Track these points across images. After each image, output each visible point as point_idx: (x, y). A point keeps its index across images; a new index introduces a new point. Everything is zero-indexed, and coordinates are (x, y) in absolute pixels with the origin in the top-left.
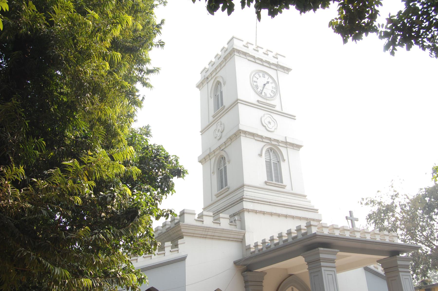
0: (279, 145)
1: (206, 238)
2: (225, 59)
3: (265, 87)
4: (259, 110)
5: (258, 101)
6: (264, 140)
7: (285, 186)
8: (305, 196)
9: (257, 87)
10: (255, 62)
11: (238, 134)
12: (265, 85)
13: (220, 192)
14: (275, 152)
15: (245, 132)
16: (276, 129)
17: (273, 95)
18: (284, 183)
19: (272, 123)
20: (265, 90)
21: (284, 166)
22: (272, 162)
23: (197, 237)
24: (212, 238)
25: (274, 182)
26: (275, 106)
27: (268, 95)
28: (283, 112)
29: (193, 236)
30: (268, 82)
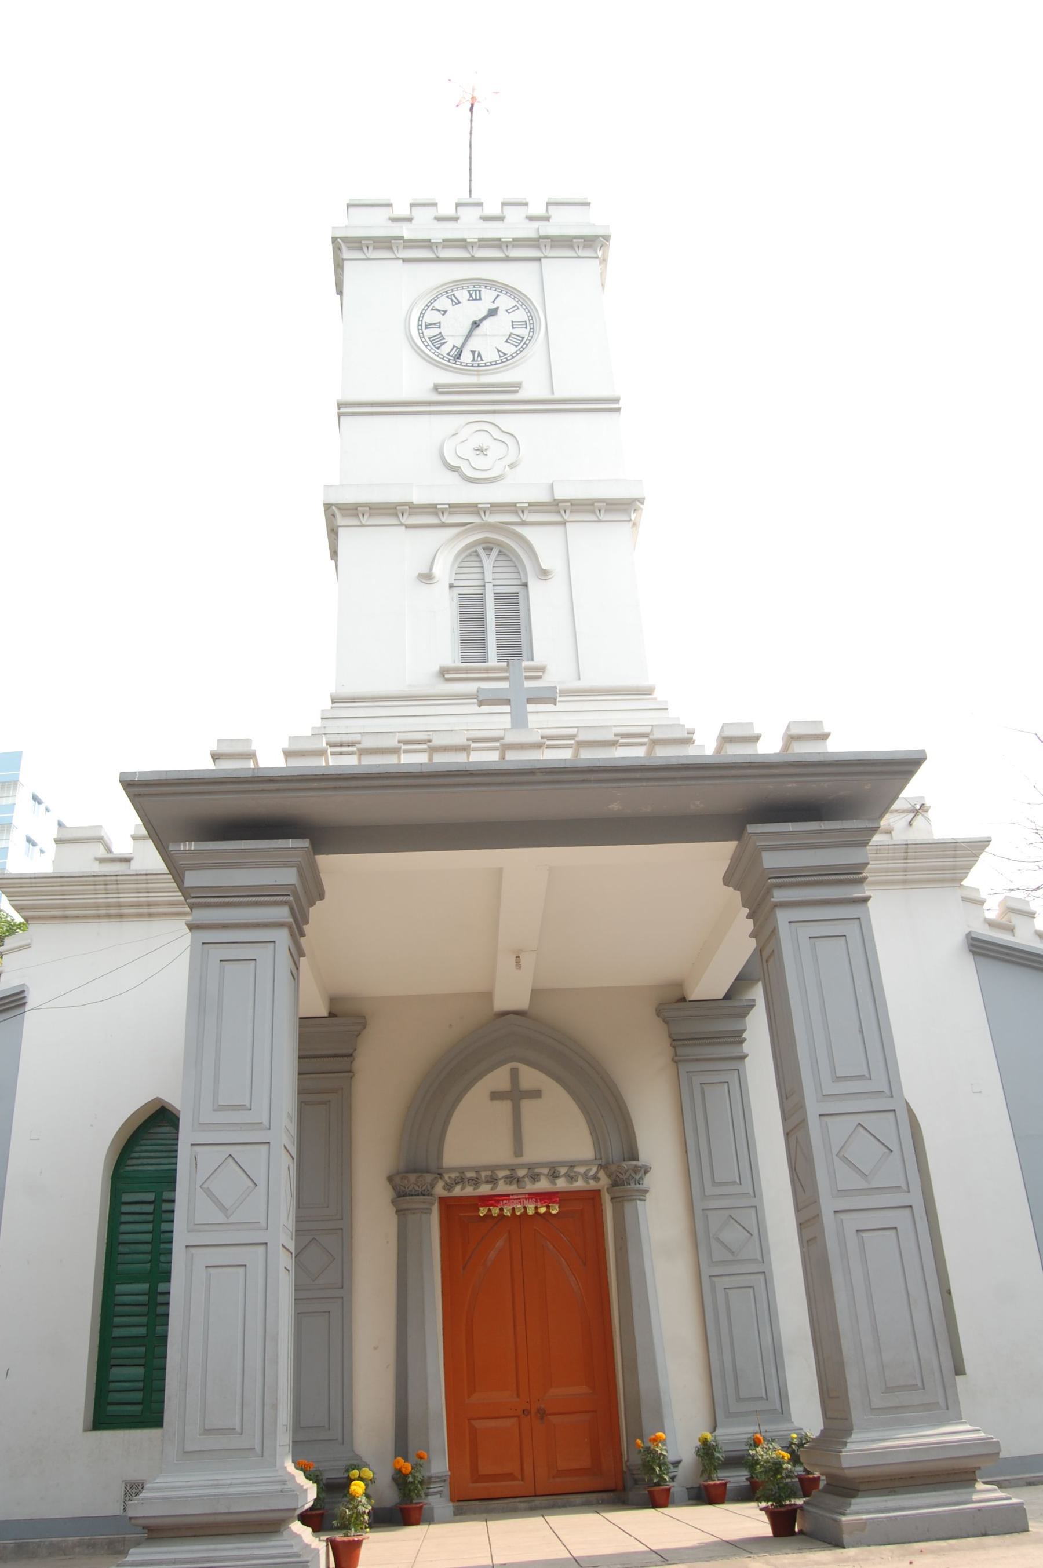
0: (523, 523)
1: (121, 916)
3: (478, 331)
4: (433, 417)
5: (436, 388)
6: (447, 519)
7: (542, 669)
8: (648, 691)
9: (438, 341)
10: (438, 260)
12: (476, 324)
14: (504, 553)
16: (512, 466)
17: (509, 349)
18: (538, 660)
19: (496, 450)
20: (474, 344)
23: (85, 917)
24: (150, 915)
26: (519, 385)
27: (490, 356)
28: (558, 395)
29: (66, 917)
30: (493, 312)
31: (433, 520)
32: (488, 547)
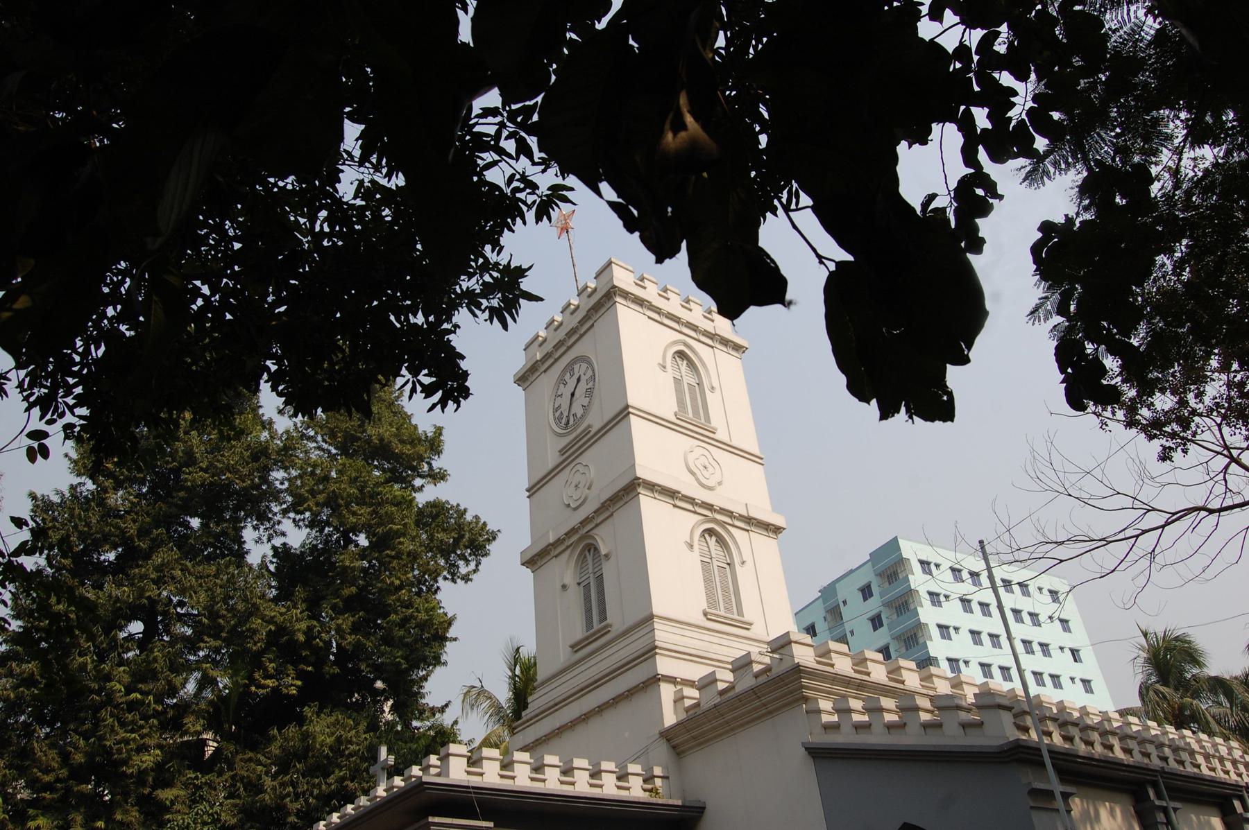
2: (596, 308)
11: (631, 488)
13: (587, 638)
14: (721, 541)
15: (651, 486)
16: (720, 483)
21: (744, 575)
22: (716, 563)
25: (722, 613)
31: (690, 507)
32: (710, 532)
